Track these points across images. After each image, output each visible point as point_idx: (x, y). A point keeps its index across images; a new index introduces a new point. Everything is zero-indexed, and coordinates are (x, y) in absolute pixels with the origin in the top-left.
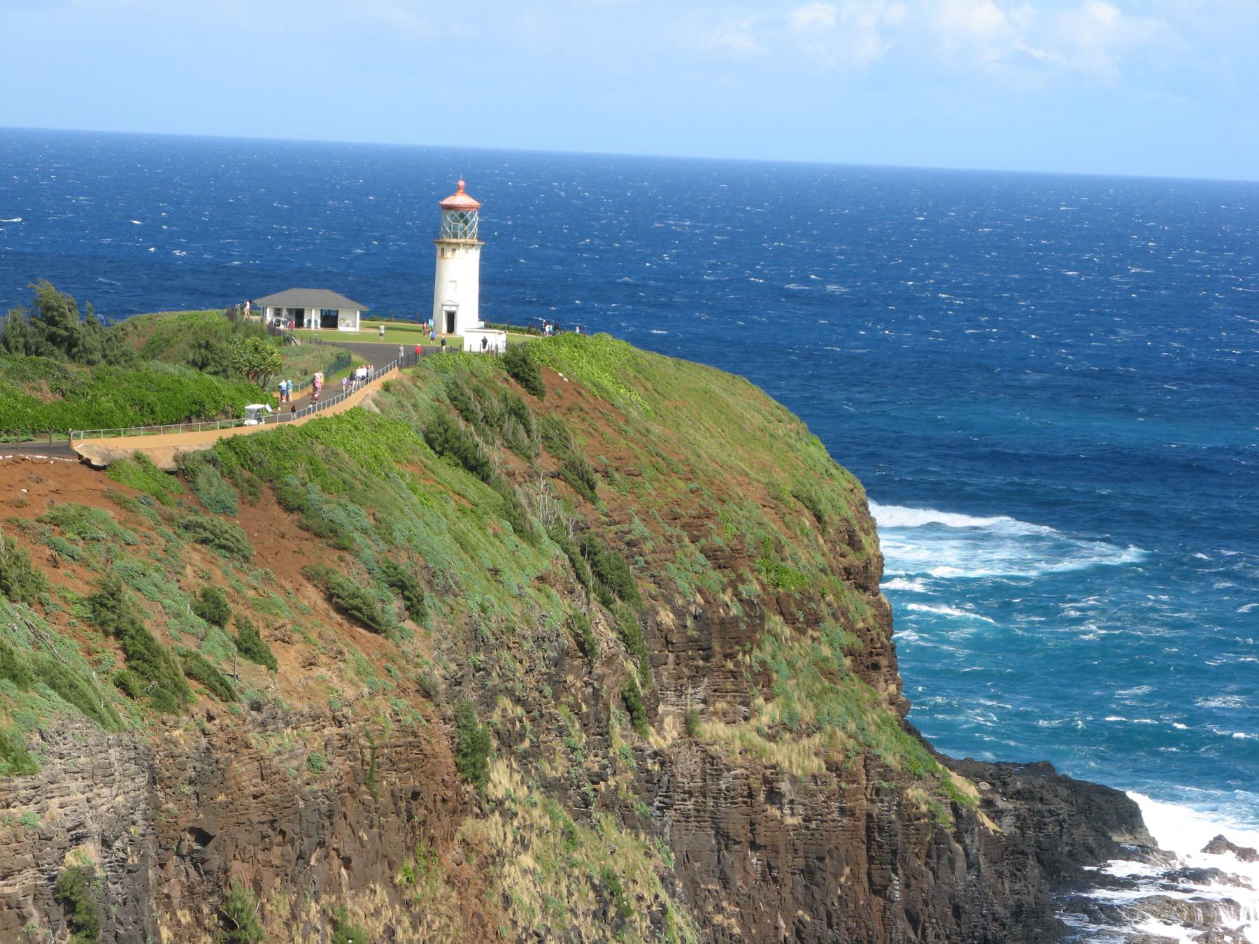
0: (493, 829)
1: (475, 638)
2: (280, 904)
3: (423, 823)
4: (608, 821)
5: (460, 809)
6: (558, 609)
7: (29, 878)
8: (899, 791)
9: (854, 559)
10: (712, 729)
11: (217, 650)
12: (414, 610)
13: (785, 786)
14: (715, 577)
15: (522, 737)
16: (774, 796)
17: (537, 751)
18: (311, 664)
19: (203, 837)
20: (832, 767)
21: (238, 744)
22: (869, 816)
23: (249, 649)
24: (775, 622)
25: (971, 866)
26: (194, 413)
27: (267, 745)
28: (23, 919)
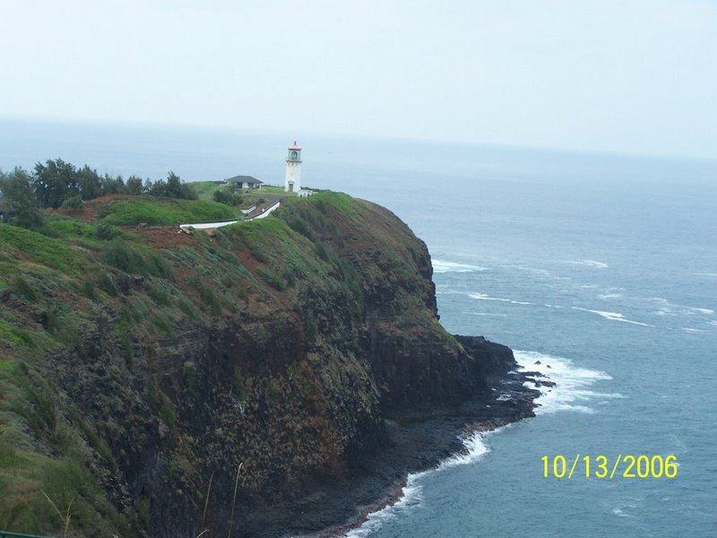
0: (314, 357)
1: (310, 293)
2: (249, 381)
3: (295, 355)
4: (352, 355)
5: (307, 349)
6: (336, 285)
7: (173, 370)
8: (441, 346)
9: (425, 269)
10: (382, 325)
11: (230, 297)
12: (291, 284)
13: (404, 343)
14: (382, 275)
15: (325, 327)
16: (400, 345)
17: (330, 331)
18: (259, 300)
19: (225, 357)
20: (420, 337)
21: (237, 328)
22: (431, 353)
23: (242, 297)
24: (402, 290)
25: (464, 370)
26: (219, 219)
27: (245, 327)
28: (171, 384)
